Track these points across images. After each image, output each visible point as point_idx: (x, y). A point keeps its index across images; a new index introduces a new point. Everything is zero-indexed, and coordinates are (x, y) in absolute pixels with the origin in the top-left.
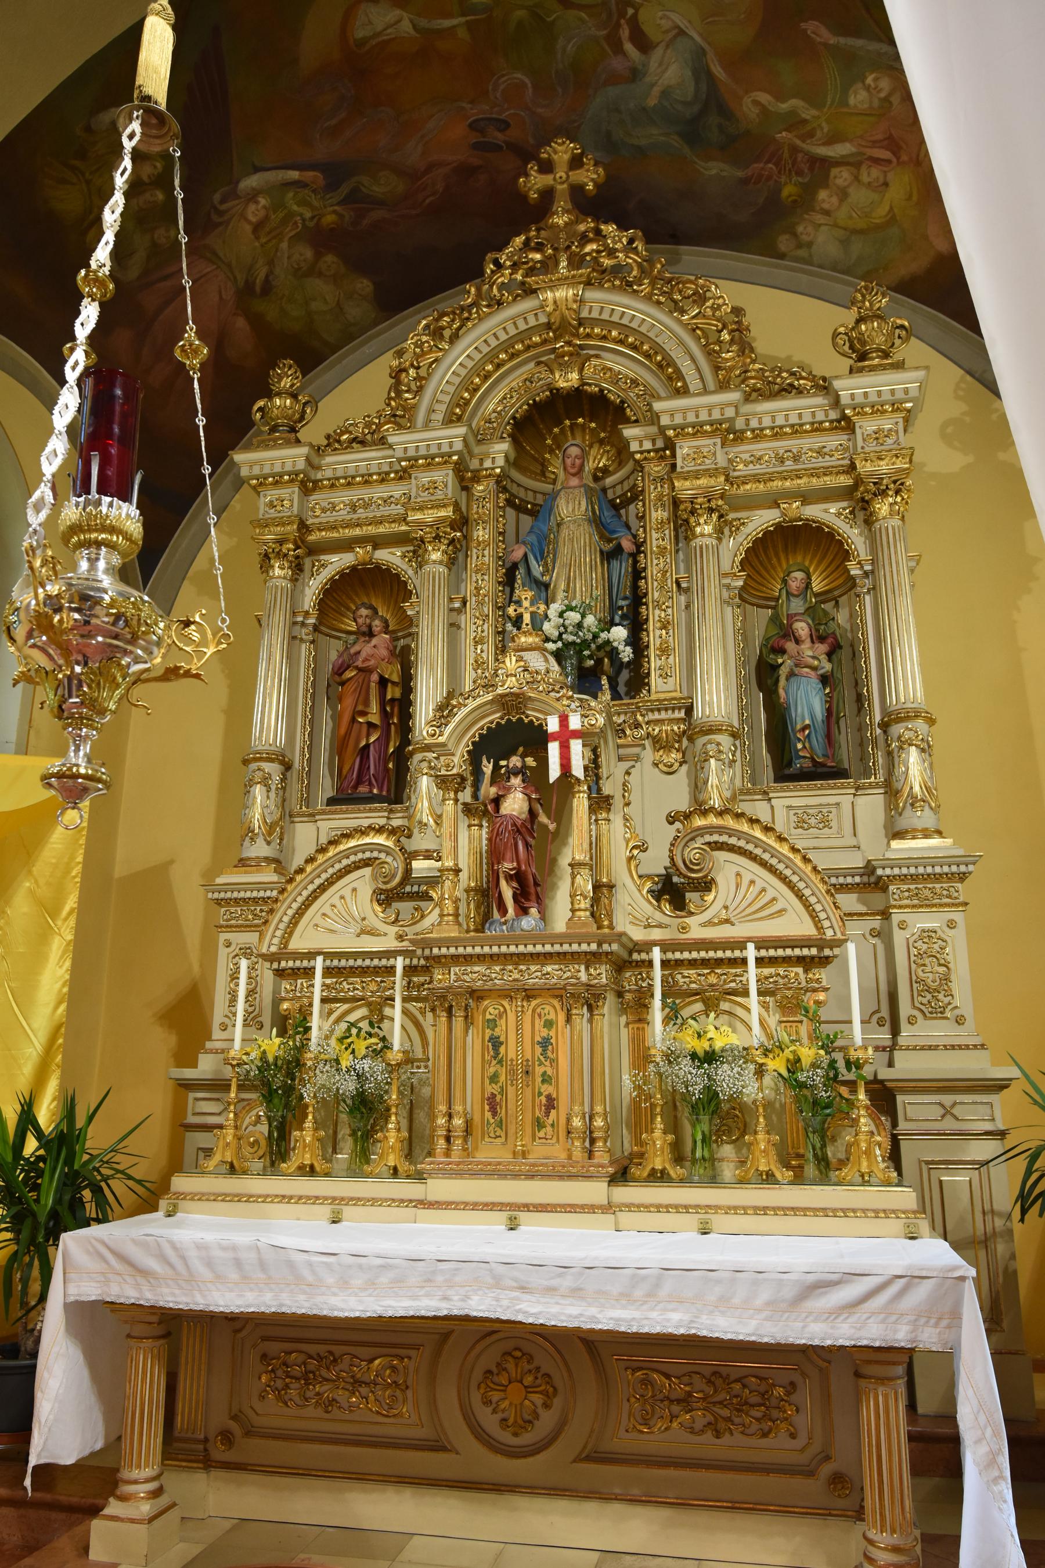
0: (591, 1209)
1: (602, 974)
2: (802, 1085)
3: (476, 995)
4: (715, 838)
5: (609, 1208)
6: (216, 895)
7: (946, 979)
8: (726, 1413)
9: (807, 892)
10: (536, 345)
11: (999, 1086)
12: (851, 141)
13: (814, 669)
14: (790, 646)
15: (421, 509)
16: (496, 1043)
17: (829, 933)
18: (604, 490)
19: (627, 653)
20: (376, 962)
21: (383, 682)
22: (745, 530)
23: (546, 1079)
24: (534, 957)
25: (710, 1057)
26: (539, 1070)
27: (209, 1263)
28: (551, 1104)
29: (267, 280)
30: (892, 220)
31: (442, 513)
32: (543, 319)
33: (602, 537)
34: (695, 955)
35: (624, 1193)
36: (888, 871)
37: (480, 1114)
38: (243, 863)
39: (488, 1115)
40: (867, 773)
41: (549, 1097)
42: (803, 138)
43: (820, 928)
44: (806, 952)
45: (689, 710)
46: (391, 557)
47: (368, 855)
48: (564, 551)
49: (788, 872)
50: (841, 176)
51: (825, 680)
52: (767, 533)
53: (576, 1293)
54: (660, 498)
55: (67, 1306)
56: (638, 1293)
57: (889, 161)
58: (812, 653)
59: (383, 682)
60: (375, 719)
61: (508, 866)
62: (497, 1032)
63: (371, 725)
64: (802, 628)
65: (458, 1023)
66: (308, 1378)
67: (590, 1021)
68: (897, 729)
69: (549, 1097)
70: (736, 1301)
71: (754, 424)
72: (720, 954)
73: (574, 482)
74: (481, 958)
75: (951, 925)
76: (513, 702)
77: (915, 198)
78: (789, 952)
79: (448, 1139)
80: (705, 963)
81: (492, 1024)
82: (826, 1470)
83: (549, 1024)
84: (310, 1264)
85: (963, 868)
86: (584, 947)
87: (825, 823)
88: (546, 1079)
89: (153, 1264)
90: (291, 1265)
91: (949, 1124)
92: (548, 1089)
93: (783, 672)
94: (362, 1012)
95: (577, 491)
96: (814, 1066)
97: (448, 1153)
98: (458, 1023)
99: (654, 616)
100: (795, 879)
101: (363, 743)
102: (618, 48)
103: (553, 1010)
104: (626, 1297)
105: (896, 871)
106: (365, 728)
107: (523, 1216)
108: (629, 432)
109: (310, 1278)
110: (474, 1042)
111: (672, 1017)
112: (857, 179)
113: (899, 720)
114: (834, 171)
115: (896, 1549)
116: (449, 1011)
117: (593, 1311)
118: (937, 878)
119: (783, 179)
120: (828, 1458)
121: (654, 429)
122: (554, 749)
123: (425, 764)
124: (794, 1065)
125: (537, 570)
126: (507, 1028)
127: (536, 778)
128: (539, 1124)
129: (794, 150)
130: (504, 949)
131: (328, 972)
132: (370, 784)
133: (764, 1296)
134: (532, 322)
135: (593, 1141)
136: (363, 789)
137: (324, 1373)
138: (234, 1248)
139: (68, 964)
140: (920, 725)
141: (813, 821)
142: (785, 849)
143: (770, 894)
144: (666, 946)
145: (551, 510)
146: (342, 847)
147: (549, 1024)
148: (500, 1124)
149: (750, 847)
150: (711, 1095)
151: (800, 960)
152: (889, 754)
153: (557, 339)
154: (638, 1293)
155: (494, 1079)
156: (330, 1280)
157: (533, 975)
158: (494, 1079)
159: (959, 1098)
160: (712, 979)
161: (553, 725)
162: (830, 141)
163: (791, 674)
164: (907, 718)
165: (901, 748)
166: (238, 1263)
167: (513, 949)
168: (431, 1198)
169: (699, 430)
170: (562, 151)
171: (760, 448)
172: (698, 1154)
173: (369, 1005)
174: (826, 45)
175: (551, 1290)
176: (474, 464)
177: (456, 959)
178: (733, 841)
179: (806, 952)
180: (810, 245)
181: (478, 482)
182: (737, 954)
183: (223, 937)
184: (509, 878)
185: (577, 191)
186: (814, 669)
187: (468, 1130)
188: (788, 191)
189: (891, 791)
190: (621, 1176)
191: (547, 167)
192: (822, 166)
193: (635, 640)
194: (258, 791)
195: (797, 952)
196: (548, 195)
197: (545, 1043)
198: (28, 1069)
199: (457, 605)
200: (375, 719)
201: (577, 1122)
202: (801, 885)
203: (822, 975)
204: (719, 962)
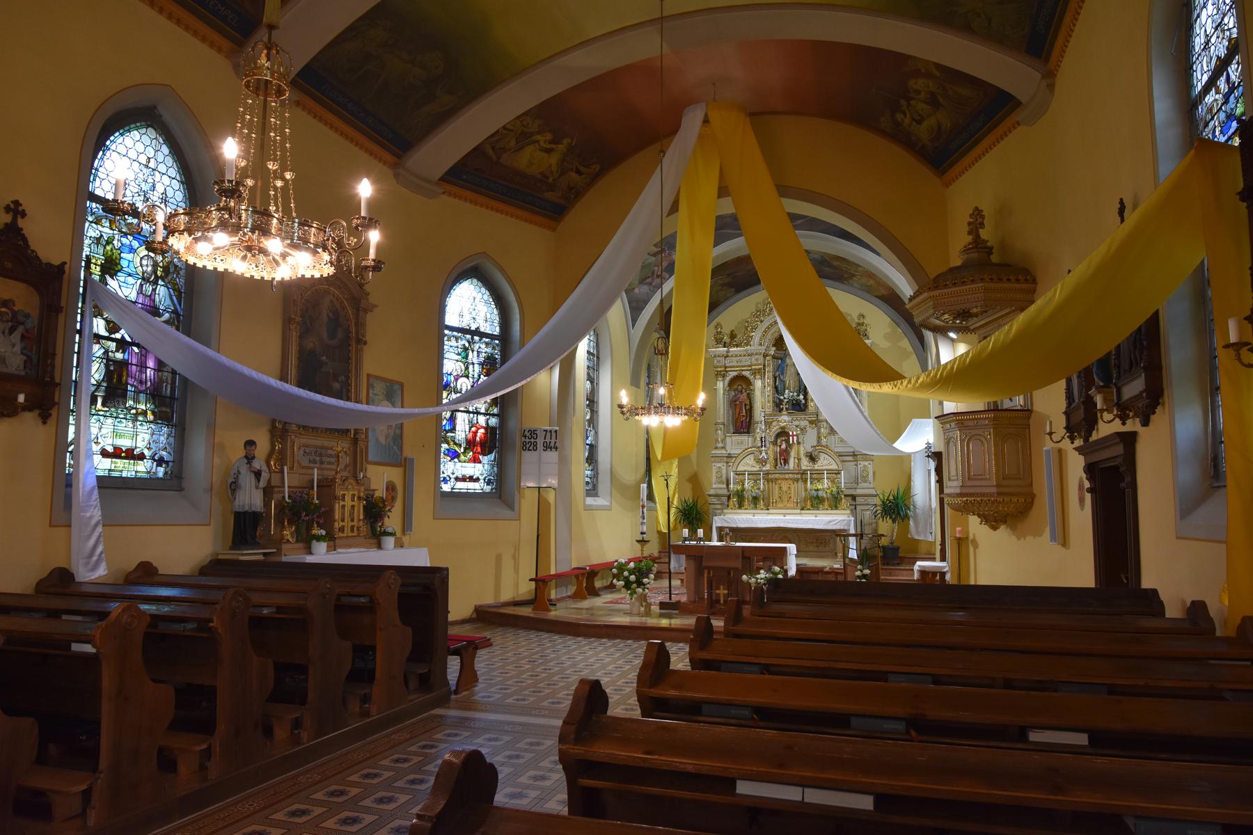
1: (799, 476)
3: (777, 479)
5: (800, 514)
19: (803, 402)
21: (745, 405)
24: (785, 473)
25: (818, 490)
27: (739, 520)
28: (790, 498)
31: (760, 367)
35: (803, 512)
37: (778, 499)
38: (716, 448)
45: (817, 415)
46: (746, 374)
48: (789, 372)
55: (716, 527)
59: (745, 405)
60: (744, 414)
61: (783, 457)
63: (743, 416)
65: (774, 484)
76: (783, 428)
81: (780, 484)
89: (729, 521)
98: (774, 484)
103: (790, 482)
110: (777, 487)
111: (811, 483)
122: (791, 438)
124: (832, 491)
126: (782, 485)
127: (787, 441)
136: (742, 430)
144: (810, 470)
150: (817, 496)
157: (787, 476)
161: (791, 433)
162: (856, 272)
166: (744, 520)
183: (714, 464)
187: (776, 501)
190: (802, 509)
192: (854, 275)
193: (805, 398)
194: (719, 432)
203: (839, 476)
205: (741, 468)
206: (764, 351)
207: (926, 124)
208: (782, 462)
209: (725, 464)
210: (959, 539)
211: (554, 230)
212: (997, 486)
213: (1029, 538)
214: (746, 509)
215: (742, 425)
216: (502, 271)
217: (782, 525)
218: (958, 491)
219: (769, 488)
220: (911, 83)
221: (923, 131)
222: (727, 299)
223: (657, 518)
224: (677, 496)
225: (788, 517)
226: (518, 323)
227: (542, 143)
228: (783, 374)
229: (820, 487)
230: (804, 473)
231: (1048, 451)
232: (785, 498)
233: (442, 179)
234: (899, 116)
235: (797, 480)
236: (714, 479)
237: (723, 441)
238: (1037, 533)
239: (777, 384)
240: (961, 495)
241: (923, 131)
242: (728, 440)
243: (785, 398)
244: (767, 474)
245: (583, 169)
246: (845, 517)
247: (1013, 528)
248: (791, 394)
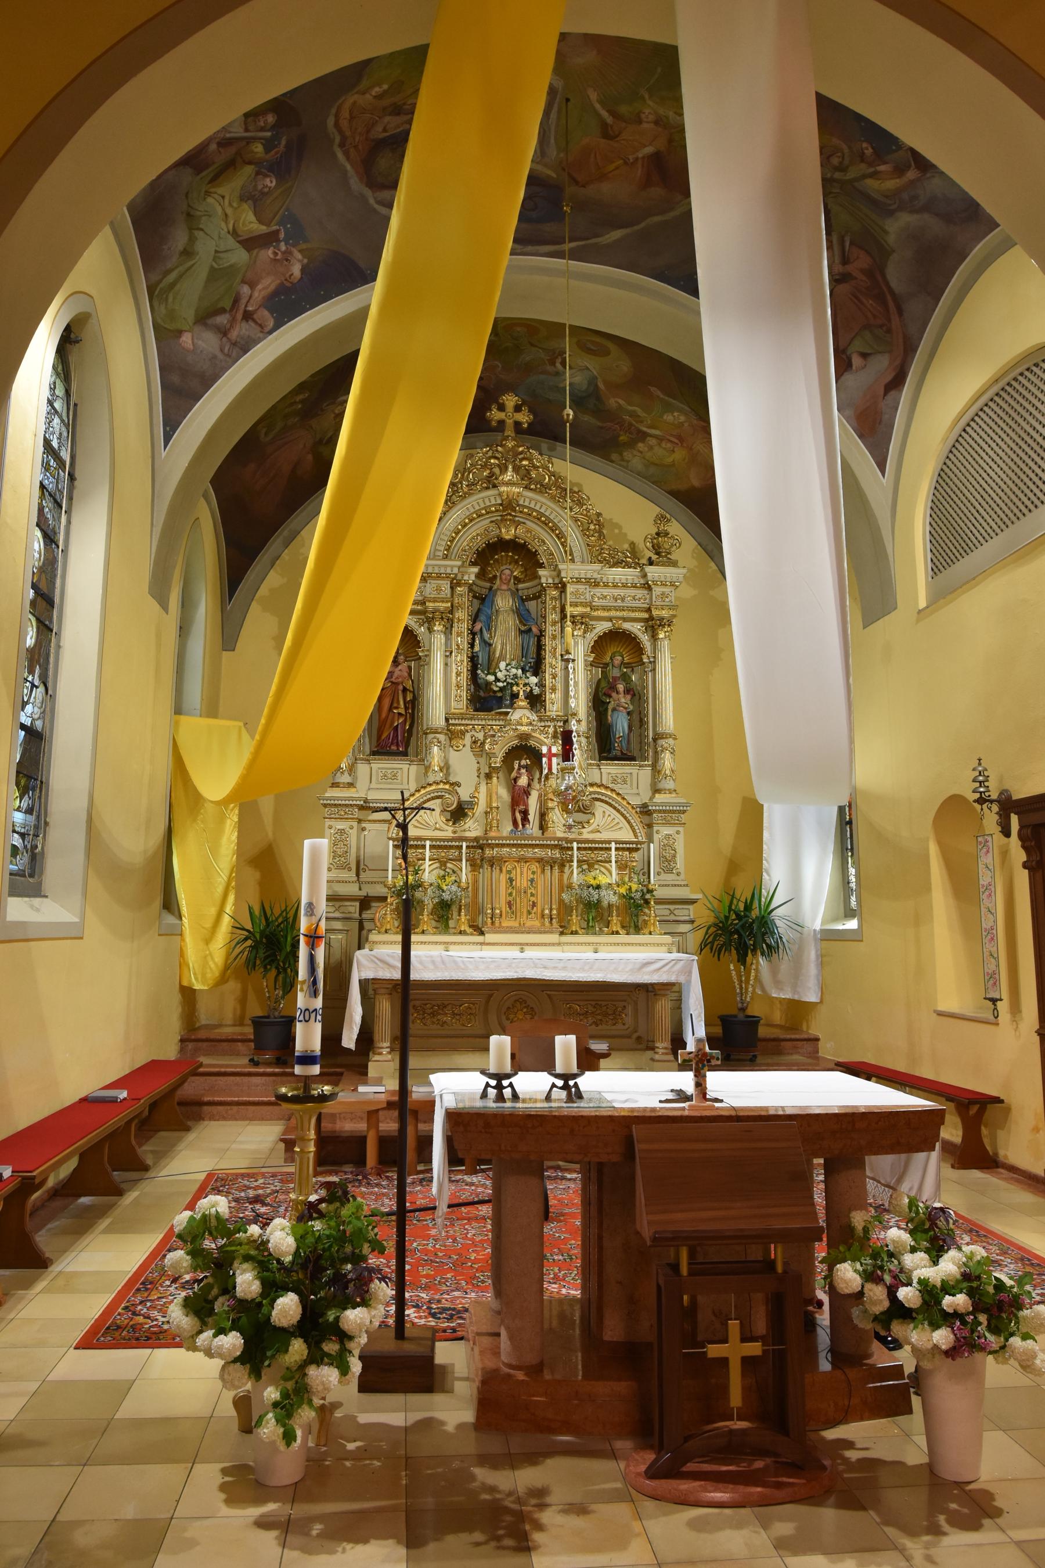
0: (553, 944)
2: (632, 898)
4: (596, 796)
5: (559, 944)
6: (325, 802)
7: (674, 856)
8: (599, 1017)
9: (632, 821)
10: (492, 512)
11: (693, 902)
12: (661, 431)
13: (626, 708)
14: (614, 695)
15: (434, 601)
16: (511, 880)
17: (640, 838)
18: (517, 590)
20: (446, 843)
21: (405, 690)
22: (596, 631)
23: (532, 895)
24: (526, 846)
25: (598, 887)
26: (529, 891)
28: (534, 905)
29: (331, 437)
30: (673, 464)
32: (499, 502)
33: (521, 622)
34: (587, 845)
36: (654, 808)
37: (505, 908)
38: (335, 785)
39: (508, 909)
40: (646, 759)
41: (533, 902)
42: (637, 422)
43: (636, 836)
44: (631, 846)
47: (440, 794)
49: (625, 812)
50: (653, 442)
51: (629, 713)
52: (605, 633)
53: (564, 968)
54: (554, 608)
56: (586, 968)
57: (677, 444)
59: (405, 690)
60: (403, 712)
62: (512, 875)
63: (400, 714)
64: (621, 687)
65: (496, 872)
66: (433, 1014)
67: (551, 872)
68: (661, 742)
69: (533, 902)
70: (620, 969)
71: (604, 580)
72: (597, 845)
73: (504, 587)
74: (508, 845)
75: (678, 832)
77: (686, 461)
78: (624, 846)
79: (492, 918)
80: (590, 849)
81: (509, 872)
82: (635, 1036)
83: (534, 873)
84: (463, 962)
85: (685, 808)
86: (552, 842)
87: (625, 782)
88: (532, 895)
90: (455, 962)
91: (672, 918)
92: (532, 899)
93: (610, 707)
94: (437, 865)
95: (506, 593)
96: (637, 891)
97: (493, 923)
99: (548, 671)
100: (628, 815)
101: (396, 724)
102: (553, 364)
103: (536, 866)
104: (582, 970)
105: (657, 808)
106: (396, 715)
107: (526, 947)
108: (542, 572)
109: (463, 966)
110: (503, 878)
112: (659, 444)
113: (662, 738)
114: (648, 438)
115: (666, 1048)
116: (492, 866)
117: (570, 974)
118: (674, 812)
119: (621, 433)
120: (636, 1032)
121: (555, 573)
122: (544, 760)
123: (435, 740)
125: (486, 636)
128: (529, 913)
129: (631, 424)
130: (519, 842)
131: (432, 847)
132: (398, 745)
133: (630, 967)
134: (493, 502)
135: (552, 919)
136: (394, 748)
137: (441, 1012)
138: (431, 957)
139: (236, 834)
140: (671, 741)
141: (619, 781)
142: (625, 803)
143: (617, 821)
145: (493, 602)
146: (428, 789)
147: (534, 873)
148: (513, 913)
149: (610, 801)
151: (628, 849)
152: (656, 753)
153: (504, 511)
154: (586, 968)
155: (510, 894)
156: (471, 967)
157: (529, 853)
158: (510, 894)
159: (677, 907)
160: (593, 855)
161: (545, 750)
162: (649, 427)
163: (614, 710)
164: (666, 738)
165: (662, 751)
166: (433, 962)
167: (523, 842)
168: (487, 941)
169: (579, 581)
170: (510, 400)
171: (606, 591)
172: (590, 924)
173: (440, 862)
174: (658, 397)
175: (555, 968)
176: (459, 577)
177: (497, 845)
178: (603, 798)
179: (631, 846)
180: (628, 461)
181: (460, 586)
182: (607, 846)
183: (328, 822)
184: (520, 812)
185: (517, 424)
186: (626, 708)
188: (623, 438)
189: (656, 770)
191: (502, 408)
192: (643, 436)
195: (628, 846)
196: (501, 422)
197: (532, 881)
198: (220, 890)
199: (448, 654)
200: (403, 712)
201: (547, 912)
202: (630, 818)
204: (596, 849)
206: (456, 570)
208: (519, 817)
209: (355, 824)
214: (423, 932)
215: (396, 736)
217: (530, 974)
219: (476, 882)
223: (182, 954)
224: (231, 898)
225: (531, 953)
228: (489, 629)
229: (603, 880)
230: (564, 847)
232: (522, 905)
235: (552, 863)
237: (351, 769)
239: (477, 648)
242: (362, 769)
243: (497, 680)
244: (478, 845)
246: (662, 955)
248: (514, 671)
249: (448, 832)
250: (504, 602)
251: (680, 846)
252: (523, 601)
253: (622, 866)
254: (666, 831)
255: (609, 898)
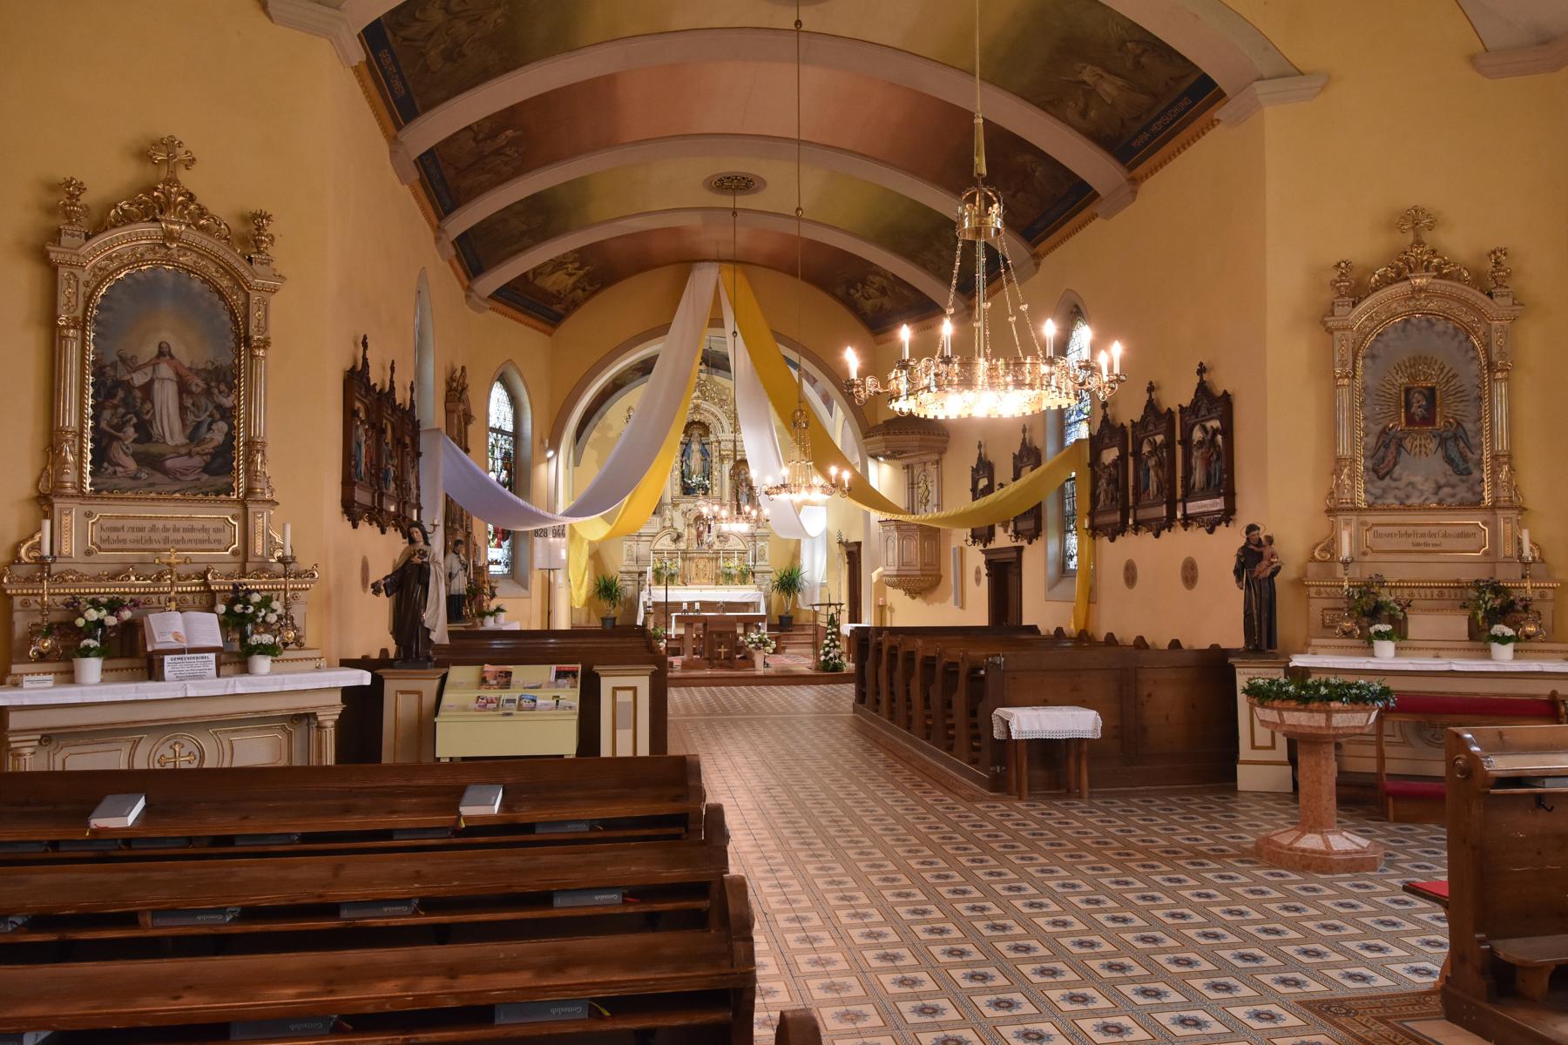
58: (745, 490)
110: (694, 565)
157: (704, 555)
205: (658, 547)
207: (870, 302)
210: (881, 606)
211: (550, 335)
212: (921, 570)
213: (937, 605)
216: (521, 376)
218: (895, 573)
220: (870, 277)
221: (868, 305)
222: (632, 381)
225: (704, 592)
226: (530, 422)
227: (569, 270)
229: (732, 565)
230: (717, 552)
231: (955, 549)
232: (701, 574)
233: (490, 297)
234: (852, 291)
235: (712, 559)
236: (625, 557)
238: (943, 600)
240: (897, 576)
241: (868, 305)
244: (684, 552)
245: (588, 288)
246: (753, 592)
247: (924, 598)
249: (673, 547)
250: (695, 447)
251: (767, 550)
252: (703, 445)
253: (740, 560)
254: (762, 544)
255: (734, 572)
